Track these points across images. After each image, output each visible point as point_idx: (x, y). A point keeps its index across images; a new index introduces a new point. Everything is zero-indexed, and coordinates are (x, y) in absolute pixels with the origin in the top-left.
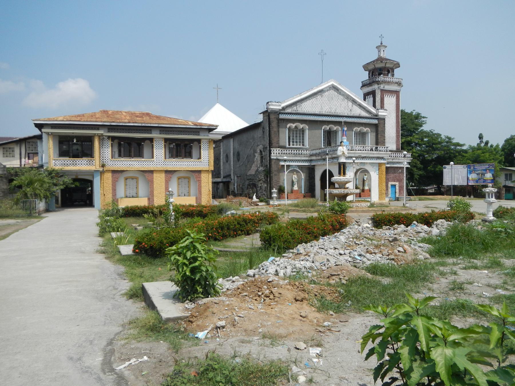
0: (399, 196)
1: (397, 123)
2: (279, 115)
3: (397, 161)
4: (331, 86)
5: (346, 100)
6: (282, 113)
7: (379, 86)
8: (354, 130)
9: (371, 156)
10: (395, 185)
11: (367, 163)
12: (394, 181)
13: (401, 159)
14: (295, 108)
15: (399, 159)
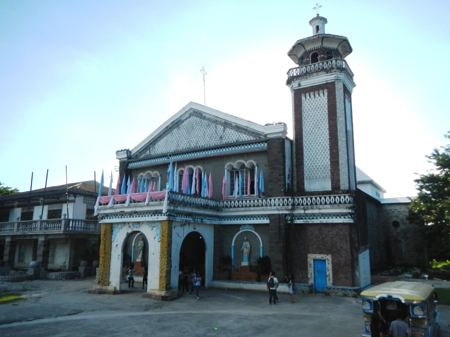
0: (334, 284)
1: (330, 139)
2: (127, 165)
3: (316, 211)
4: (192, 111)
5: (213, 125)
6: (132, 162)
7: (291, 86)
8: (226, 167)
9: (138, 209)
10: (324, 261)
11: (143, 222)
12: (320, 253)
13: (324, 208)
14: (148, 152)
15: (320, 209)
